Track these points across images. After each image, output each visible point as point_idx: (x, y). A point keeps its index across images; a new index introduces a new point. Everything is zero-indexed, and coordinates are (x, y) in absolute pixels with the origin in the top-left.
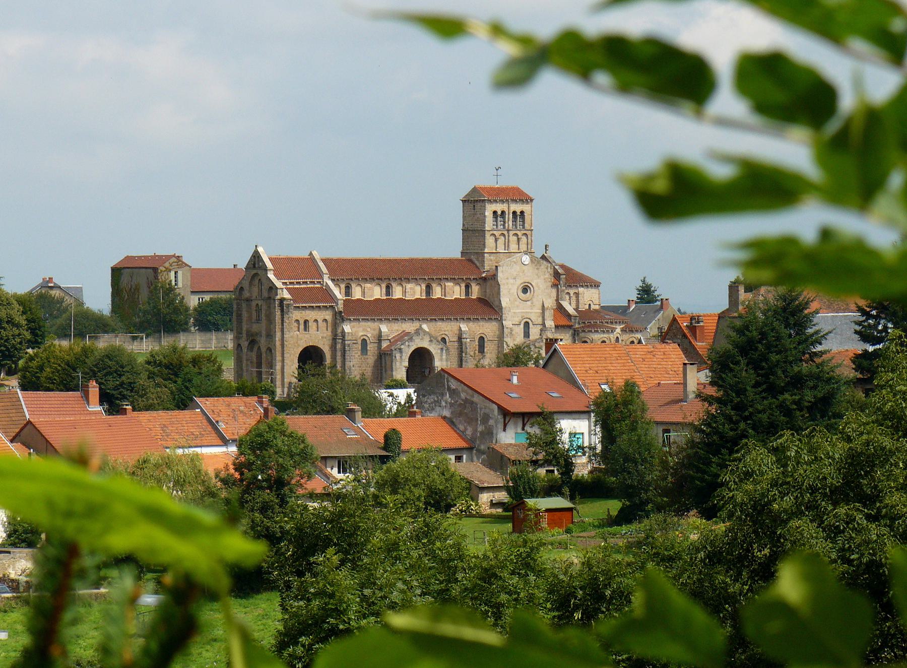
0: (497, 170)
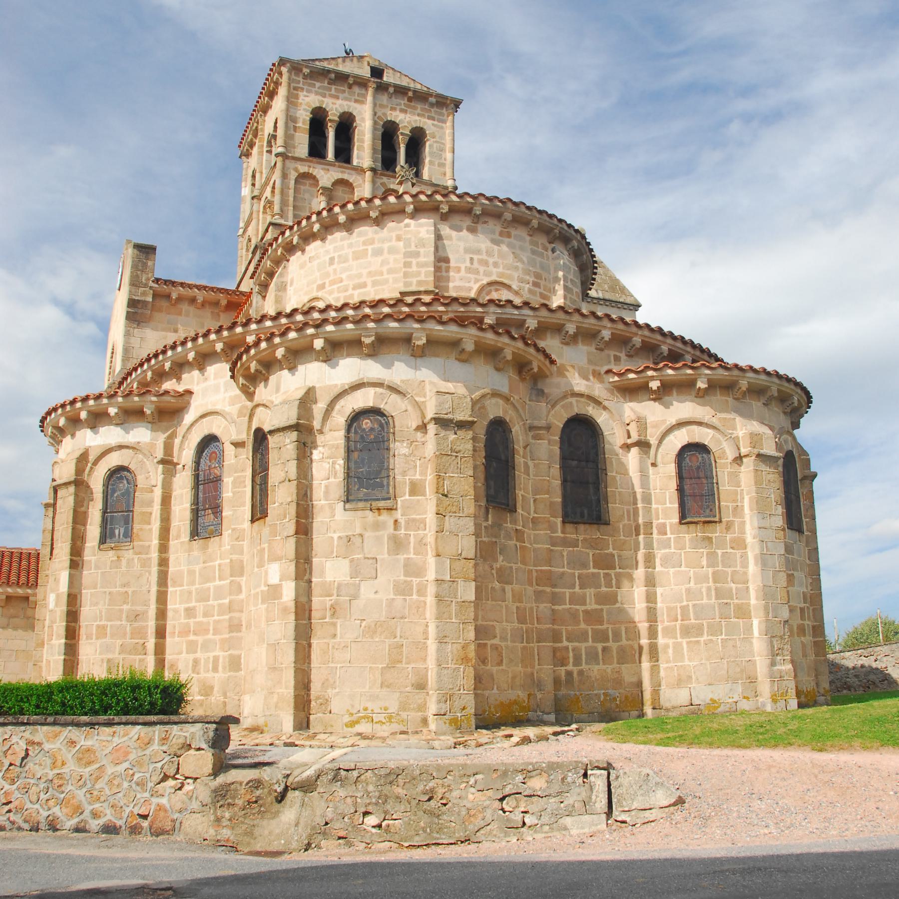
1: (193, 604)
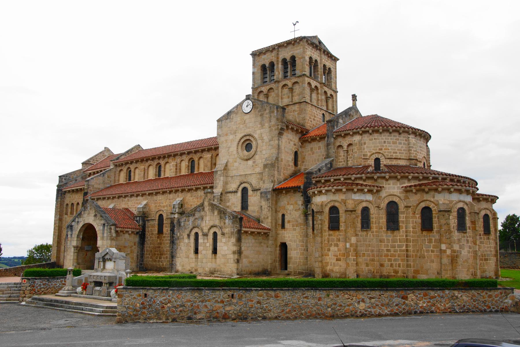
0: (294, 25)
1: (389, 248)
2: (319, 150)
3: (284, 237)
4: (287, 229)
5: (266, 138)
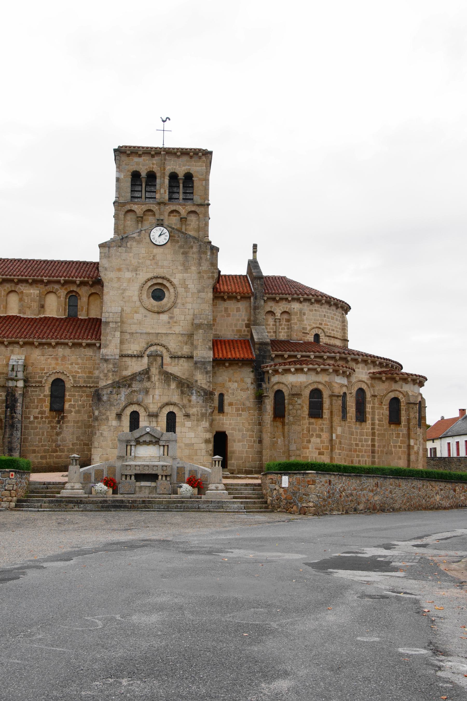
0: (164, 121)
1: (358, 442)
2: (237, 312)
3: (223, 424)
4: (228, 413)
5: (192, 287)
